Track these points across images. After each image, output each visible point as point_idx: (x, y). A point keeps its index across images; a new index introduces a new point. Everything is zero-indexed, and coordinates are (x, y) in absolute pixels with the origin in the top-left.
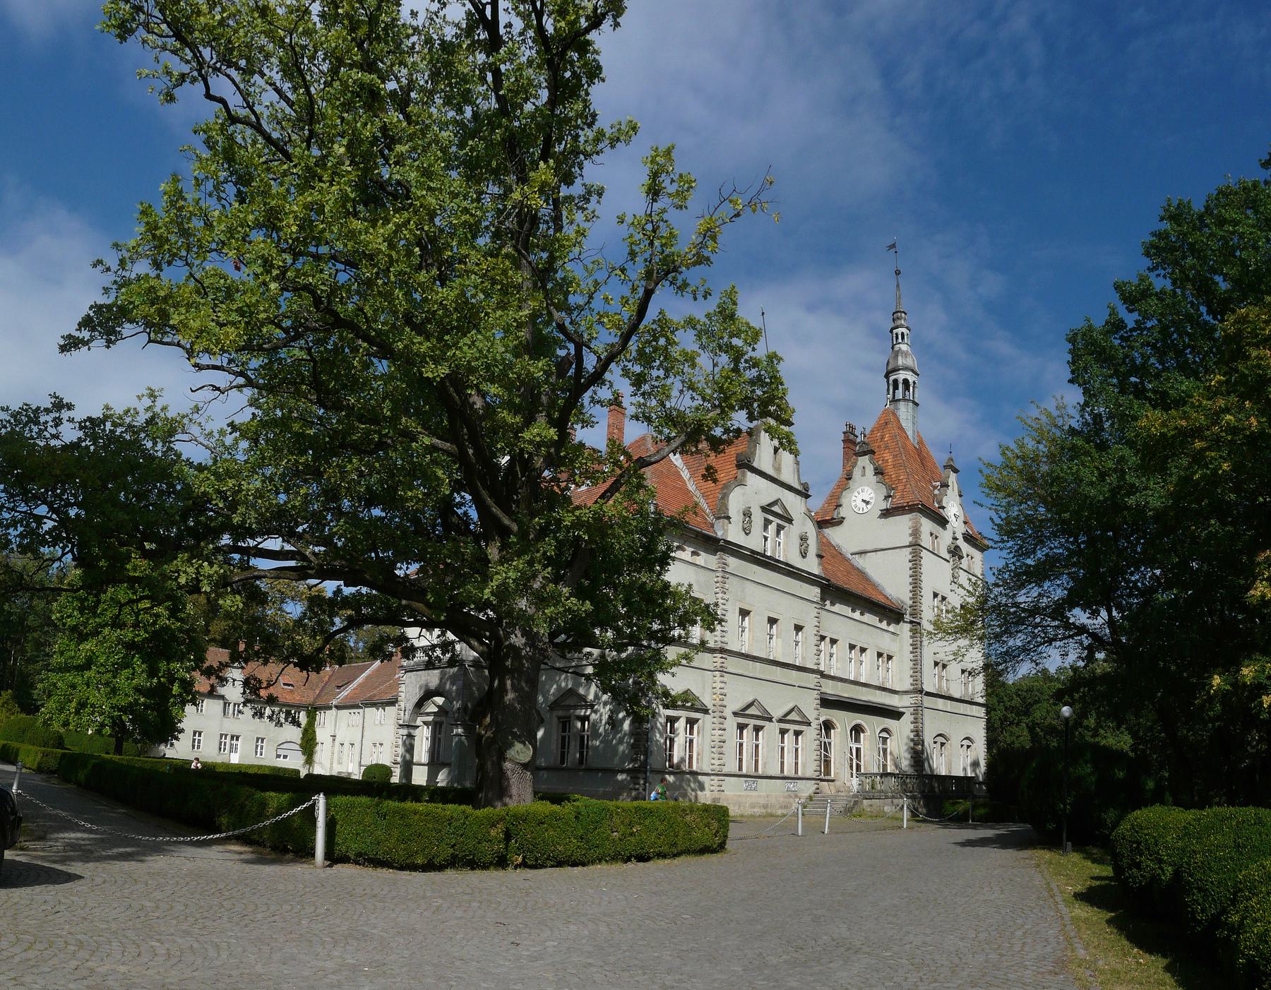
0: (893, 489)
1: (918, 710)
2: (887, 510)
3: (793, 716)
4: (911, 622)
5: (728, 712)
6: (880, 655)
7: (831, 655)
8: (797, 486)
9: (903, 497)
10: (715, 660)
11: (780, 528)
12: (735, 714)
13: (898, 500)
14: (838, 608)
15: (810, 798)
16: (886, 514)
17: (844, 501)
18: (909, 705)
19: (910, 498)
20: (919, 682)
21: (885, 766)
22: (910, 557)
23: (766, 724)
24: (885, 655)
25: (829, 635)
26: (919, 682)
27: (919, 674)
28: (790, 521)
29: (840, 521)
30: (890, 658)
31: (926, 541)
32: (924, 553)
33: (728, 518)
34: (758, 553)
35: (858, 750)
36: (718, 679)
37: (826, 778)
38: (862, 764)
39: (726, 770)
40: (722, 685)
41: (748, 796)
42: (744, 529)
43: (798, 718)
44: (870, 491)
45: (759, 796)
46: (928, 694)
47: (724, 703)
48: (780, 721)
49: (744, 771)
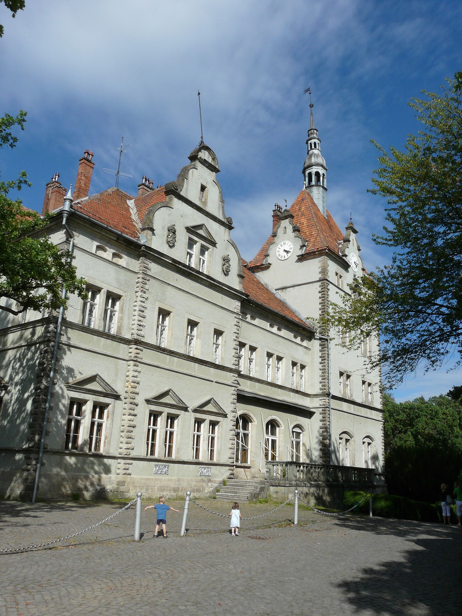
0: (307, 241)
1: (326, 409)
2: (302, 255)
3: (209, 408)
4: (320, 339)
5: (140, 399)
6: (294, 364)
7: (251, 361)
8: (221, 217)
9: (314, 246)
10: (130, 350)
11: (203, 250)
12: (148, 401)
13: (311, 248)
14: (257, 321)
15: (224, 483)
16: (301, 258)
17: (271, 252)
18: (318, 406)
19: (320, 245)
20: (327, 388)
21: (298, 457)
22: (320, 289)
23: (182, 413)
24: (299, 365)
25: (249, 343)
26: (327, 388)
27: (326, 381)
28: (214, 244)
29: (268, 266)
30: (303, 367)
31: (332, 277)
32: (330, 287)
33: (152, 230)
34: (180, 263)
35: (274, 442)
36: (132, 368)
37: (243, 464)
38: (277, 455)
39: (134, 454)
40: (136, 374)
41: (156, 480)
42: (168, 242)
43: (215, 410)
44: (290, 243)
45: (169, 480)
46: (334, 397)
47: (136, 390)
48: (195, 411)
49: (156, 456)
